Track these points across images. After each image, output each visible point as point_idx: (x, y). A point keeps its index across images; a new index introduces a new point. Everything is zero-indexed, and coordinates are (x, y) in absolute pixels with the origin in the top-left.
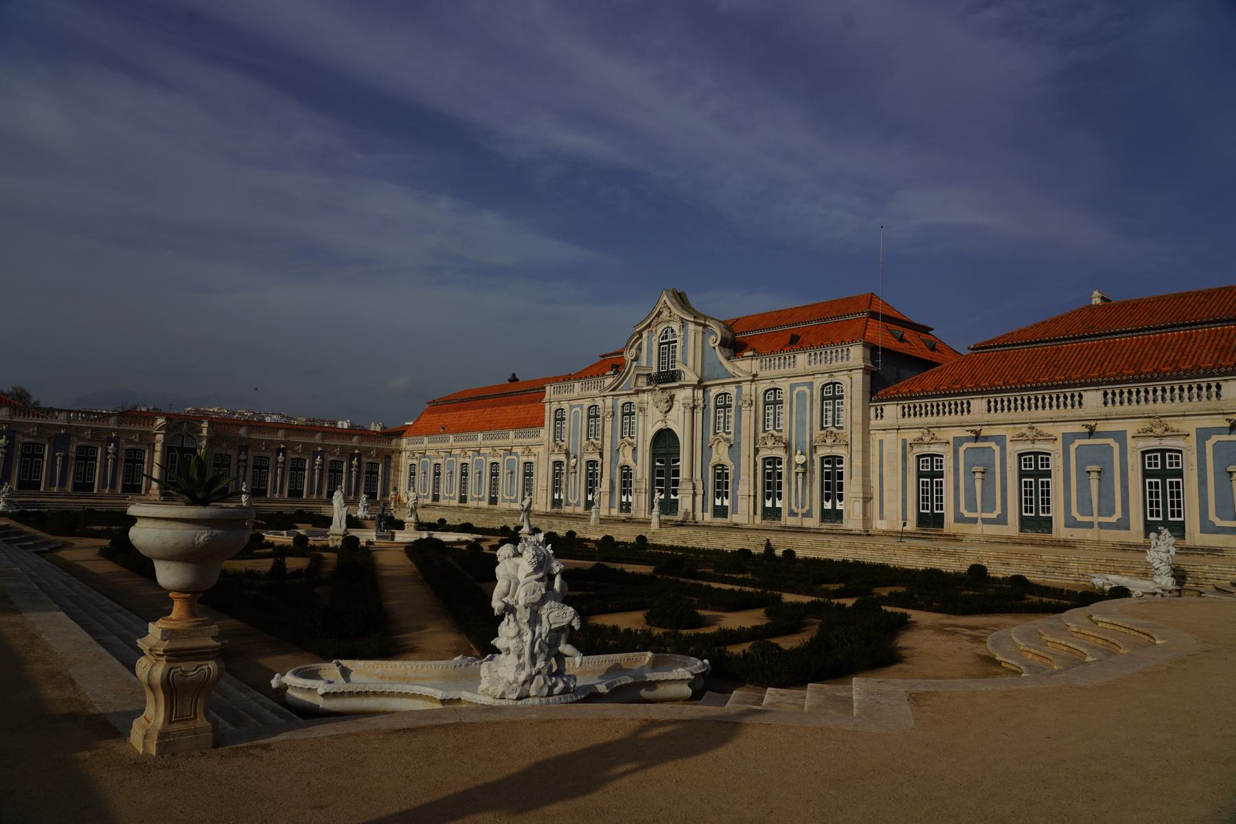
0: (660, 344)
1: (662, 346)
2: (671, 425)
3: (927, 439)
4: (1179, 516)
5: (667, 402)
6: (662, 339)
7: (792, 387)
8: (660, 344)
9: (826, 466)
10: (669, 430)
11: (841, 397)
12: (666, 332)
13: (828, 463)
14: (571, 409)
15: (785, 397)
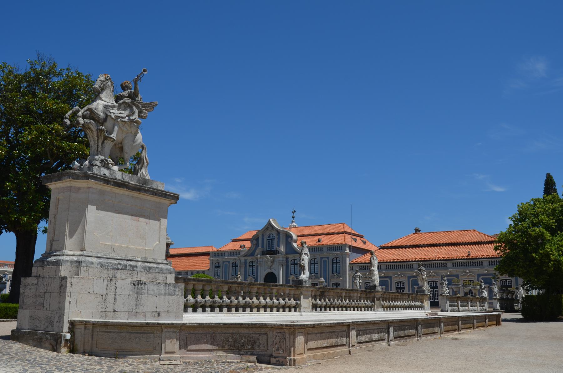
0: (267, 239)
1: (268, 240)
2: (273, 271)
4: (438, 300)
5: (272, 262)
6: (268, 237)
7: (322, 258)
8: (267, 239)
9: (334, 286)
10: (272, 273)
11: (339, 262)
12: (270, 235)
13: (335, 285)
14: (223, 262)
15: (319, 261)
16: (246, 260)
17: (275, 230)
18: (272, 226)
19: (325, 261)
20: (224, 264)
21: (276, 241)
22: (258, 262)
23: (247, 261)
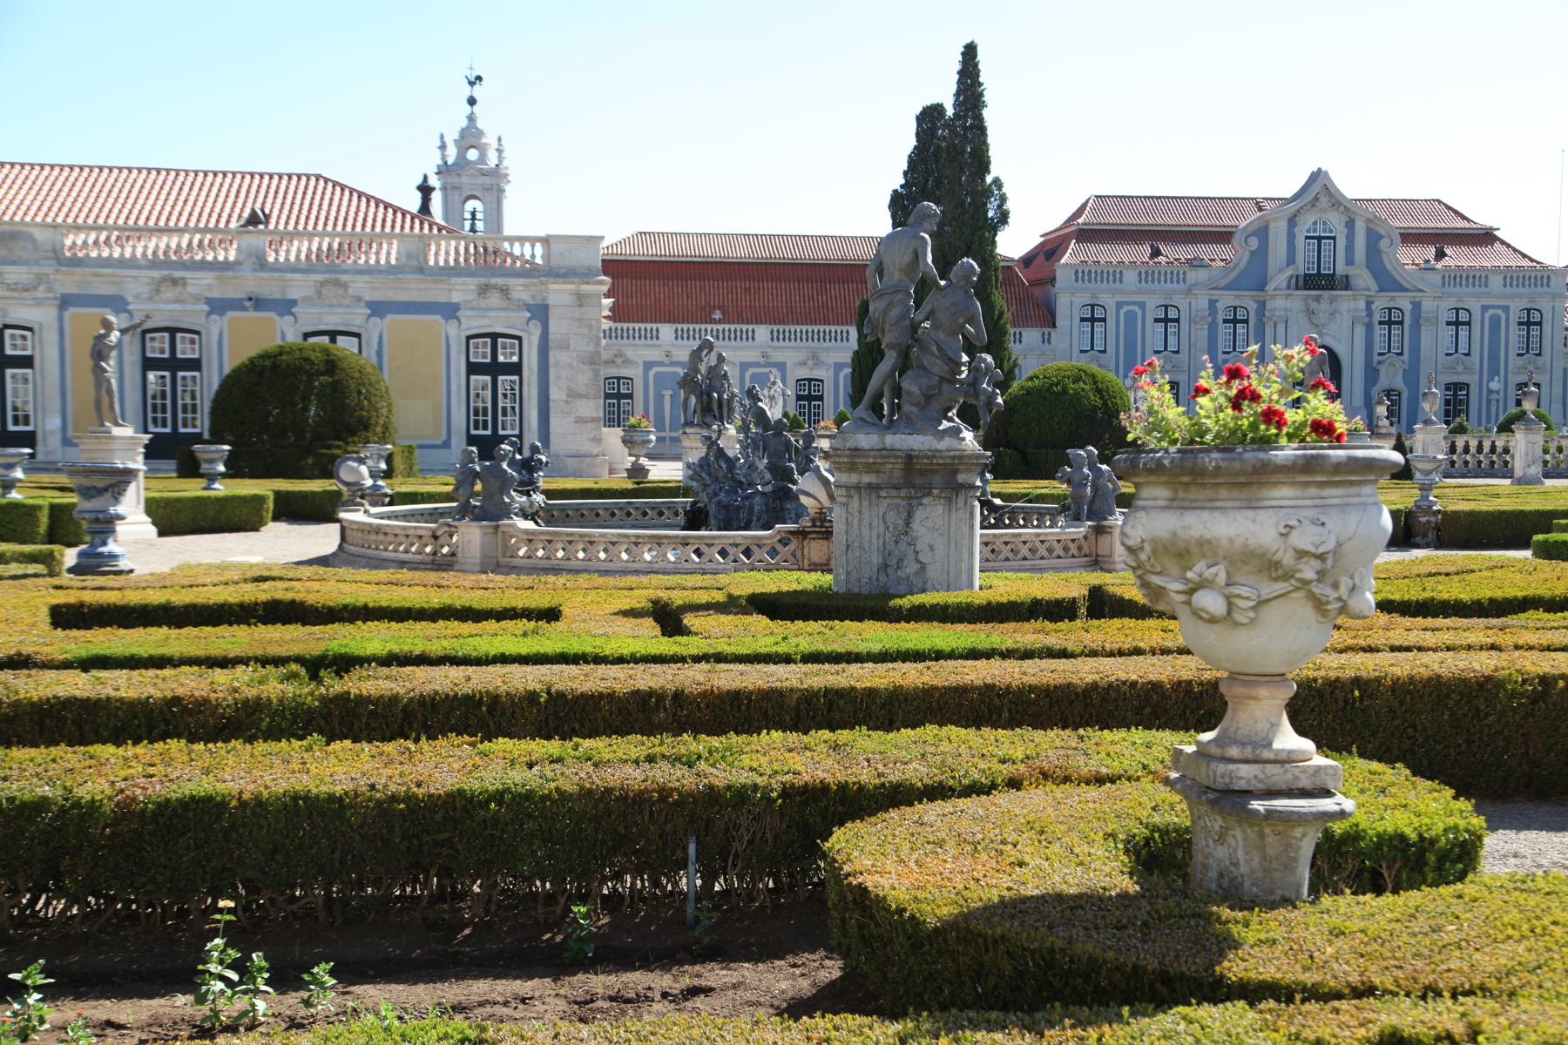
3: (1460, 368)
8: (1307, 238)
11: (1520, 324)
12: (1315, 223)
14: (1119, 305)
16: (1212, 304)
17: (1342, 208)
18: (1330, 194)
19: (1495, 322)
20: (1122, 312)
21: (1341, 243)
22: (1267, 314)
23: (1218, 305)
